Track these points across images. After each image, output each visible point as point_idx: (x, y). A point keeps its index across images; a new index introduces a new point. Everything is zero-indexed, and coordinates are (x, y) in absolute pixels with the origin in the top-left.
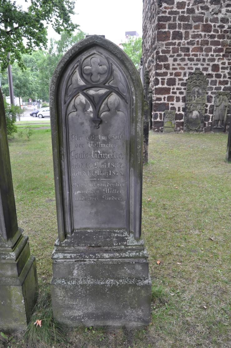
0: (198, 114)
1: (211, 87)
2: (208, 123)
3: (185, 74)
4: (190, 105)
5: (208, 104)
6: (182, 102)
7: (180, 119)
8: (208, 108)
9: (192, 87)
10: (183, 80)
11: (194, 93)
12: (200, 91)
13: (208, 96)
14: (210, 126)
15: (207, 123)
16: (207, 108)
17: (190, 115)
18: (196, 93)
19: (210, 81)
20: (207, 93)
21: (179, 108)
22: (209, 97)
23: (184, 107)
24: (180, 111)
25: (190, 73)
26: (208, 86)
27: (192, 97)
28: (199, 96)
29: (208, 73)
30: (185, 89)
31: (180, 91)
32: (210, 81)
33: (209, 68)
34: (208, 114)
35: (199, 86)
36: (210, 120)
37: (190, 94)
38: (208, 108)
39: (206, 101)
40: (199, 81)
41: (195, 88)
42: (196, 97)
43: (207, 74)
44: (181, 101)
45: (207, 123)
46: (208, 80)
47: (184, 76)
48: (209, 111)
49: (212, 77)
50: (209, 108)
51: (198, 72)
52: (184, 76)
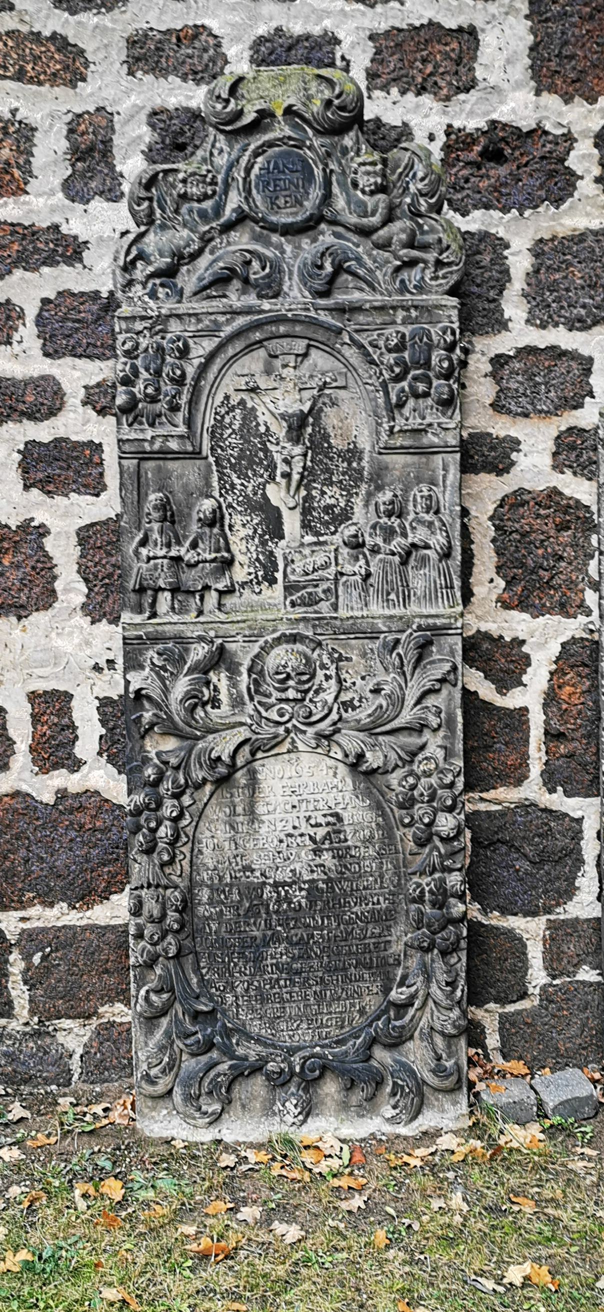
0: (358, 814)
1: (556, 353)
2: (558, 933)
3: (91, 152)
4: (198, 653)
5: (516, 624)
6: (97, 610)
7: (85, 896)
8: (529, 696)
9: (201, 349)
10: (71, 251)
11: (254, 457)
12: (354, 422)
13: (515, 501)
14: (587, 975)
15: (531, 930)
16: (513, 700)
17: (214, 837)
18: (287, 452)
19: (520, 263)
20: (482, 455)
21: (51, 706)
22: (526, 520)
23: (112, 686)
24: (75, 765)
25: (175, 135)
26: (503, 343)
27: (215, 520)
28: (332, 496)
29: (474, 123)
30: (98, 399)
31: (43, 432)
32: (520, 263)
33: (489, 41)
34: (532, 789)
35: (321, 337)
36: (588, 882)
37: (186, 473)
38: (529, 696)
39: (488, 583)
40: (308, 248)
41: (254, 363)
42: (291, 523)
43: (457, 141)
44: (71, 588)
45: (531, 930)
46: (484, 250)
47: (75, 191)
48: (552, 736)
49: (559, 185)
50: (550, 699)
51: (285, 89)
52: (75, 191)
